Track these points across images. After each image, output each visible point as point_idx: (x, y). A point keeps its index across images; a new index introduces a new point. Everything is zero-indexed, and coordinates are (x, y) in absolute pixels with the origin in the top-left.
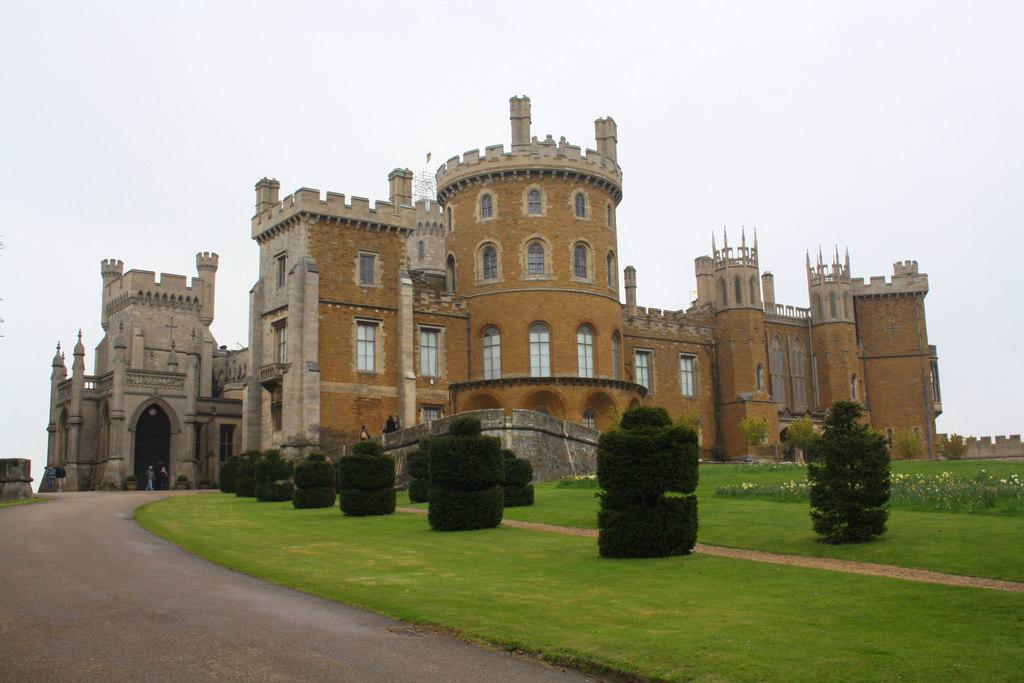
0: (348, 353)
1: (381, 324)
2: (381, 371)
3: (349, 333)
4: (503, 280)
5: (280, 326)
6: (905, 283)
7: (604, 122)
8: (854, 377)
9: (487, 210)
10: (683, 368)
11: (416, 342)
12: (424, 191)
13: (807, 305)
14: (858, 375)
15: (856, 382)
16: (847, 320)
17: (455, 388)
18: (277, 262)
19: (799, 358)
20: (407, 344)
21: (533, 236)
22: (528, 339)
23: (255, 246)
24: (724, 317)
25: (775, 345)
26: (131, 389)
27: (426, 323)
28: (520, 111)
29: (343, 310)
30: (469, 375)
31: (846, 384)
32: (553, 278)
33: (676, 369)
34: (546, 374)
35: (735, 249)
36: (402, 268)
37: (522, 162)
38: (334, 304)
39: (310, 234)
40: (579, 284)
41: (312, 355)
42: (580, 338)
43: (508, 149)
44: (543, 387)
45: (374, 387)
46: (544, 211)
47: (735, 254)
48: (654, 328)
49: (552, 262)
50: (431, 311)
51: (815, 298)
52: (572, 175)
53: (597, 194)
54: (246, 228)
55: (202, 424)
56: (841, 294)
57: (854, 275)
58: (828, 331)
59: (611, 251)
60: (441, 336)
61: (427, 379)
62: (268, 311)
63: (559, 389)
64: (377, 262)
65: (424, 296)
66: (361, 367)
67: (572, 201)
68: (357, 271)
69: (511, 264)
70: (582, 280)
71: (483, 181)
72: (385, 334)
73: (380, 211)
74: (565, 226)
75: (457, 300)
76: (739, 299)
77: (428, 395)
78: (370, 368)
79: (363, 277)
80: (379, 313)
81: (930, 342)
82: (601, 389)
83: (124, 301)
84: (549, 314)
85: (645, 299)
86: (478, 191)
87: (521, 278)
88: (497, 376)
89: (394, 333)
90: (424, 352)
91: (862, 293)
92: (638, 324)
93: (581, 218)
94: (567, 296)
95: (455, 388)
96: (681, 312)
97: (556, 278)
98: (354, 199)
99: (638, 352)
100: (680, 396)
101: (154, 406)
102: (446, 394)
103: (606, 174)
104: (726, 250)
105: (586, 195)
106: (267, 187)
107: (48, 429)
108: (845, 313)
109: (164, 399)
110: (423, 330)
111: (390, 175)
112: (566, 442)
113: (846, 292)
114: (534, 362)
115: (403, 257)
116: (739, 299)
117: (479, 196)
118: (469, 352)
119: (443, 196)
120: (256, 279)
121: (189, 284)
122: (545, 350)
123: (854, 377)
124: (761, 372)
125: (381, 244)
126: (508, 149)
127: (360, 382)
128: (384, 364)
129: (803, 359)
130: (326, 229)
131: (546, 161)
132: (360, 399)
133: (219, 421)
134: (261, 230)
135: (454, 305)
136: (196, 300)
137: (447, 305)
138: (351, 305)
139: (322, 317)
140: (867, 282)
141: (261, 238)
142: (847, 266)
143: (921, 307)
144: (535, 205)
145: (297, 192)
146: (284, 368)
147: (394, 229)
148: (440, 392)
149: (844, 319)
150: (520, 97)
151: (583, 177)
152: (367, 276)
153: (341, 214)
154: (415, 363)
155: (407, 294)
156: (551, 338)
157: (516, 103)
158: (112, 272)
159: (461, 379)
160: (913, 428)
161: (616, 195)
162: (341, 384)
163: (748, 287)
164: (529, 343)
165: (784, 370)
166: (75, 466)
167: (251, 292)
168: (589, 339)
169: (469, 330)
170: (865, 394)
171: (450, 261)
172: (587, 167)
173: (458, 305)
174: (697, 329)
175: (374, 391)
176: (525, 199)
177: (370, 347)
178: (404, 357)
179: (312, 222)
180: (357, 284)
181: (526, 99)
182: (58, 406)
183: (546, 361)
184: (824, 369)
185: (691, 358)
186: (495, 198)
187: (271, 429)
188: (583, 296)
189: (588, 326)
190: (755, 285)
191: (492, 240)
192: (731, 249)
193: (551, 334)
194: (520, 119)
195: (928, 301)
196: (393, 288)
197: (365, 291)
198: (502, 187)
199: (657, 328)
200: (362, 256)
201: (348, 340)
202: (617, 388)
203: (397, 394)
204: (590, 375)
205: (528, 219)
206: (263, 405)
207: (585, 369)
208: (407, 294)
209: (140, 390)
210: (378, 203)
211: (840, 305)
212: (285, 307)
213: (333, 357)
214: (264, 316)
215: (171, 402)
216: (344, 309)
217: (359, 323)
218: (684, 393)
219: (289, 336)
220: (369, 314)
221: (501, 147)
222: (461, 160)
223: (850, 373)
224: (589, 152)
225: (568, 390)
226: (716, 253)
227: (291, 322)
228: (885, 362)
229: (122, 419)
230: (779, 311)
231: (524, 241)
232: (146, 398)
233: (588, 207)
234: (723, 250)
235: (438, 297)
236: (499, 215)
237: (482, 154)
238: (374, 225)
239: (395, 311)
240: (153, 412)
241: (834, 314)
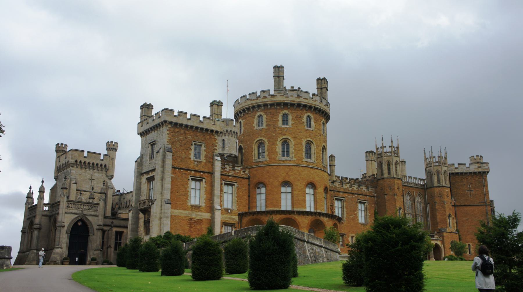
0: (186, 195)
1: (204, 180)
2: (203, 205)
3: (187, 184)
4: (268, 159)
5: (150, 180)
6: (477, 167)
7: (321, 80)
8: (450, 215)
9: (260, 123)
10: (360, 208)
11: (221, 190)
12: (228, 112)
13: (424, 177)
14: (451, 214)
15: (451, 218)
16: (446, 185)
17: (241, 215)
18: (150, 147)
19: (420, 204)
20: (217, 192)
21: (284, 137)
22: (280, 191)
23: (139, 138)
24: (381, 182)
25: (408, 197)
26: (69, 211)
27: (227, 181)
28: (279, 72)
29: (184, 171)
30: (249, 208)
31: (445, 219)
32: (294, 159)
33: (356, 209)
34: (289, 209)
35: (387, 147)
37: (279, 99)
38: (180, 169)
39: (168, 132)
40: (308, 162)
41: (167, 195)
42: (308, 190)
43: (272, 92)
44: (288, 216)
45: (198, 213)
47: (388, 150)
48: (345, 187)
49: (293, 151)
50: (230, 174)
51: (429, 174)
52: (305, 106)
53: (317, 116)
54: (135, 128)
55: (106, 230)
56: (443, 172)
57: (449, 162)
58: (436, 191)
59: (324, 146)
60: (235, 187)
61: (227, 210)
62: (144, 171)
63: (296, 217)
64: (203, 148)
65: (227, 166)
66: (192, 202)
67: (304, 120)
68: (192, 152)
69: (272, 151)
70: (309, 160)
71: (259, 109)
72: (206, 186)
73: (205, 122)
74: (300, 132)
75: (244, 169)
76: (389, 173)
77: (227, 218)
78: (197, 203)
79: (195, 155)
80: (203, 175)
81: (491, 199)
82: (318, 217)
83: (67, 165)
85: (340, 171)
86: (256, 113)
87: (277, 159)
88: (263, 209)
89: (212, 185)
90: (225, 196)
91: (453, 172)
92: (337, 184)
93: (309, 129)
94: (302, 169)
95: (241, 215)
96: (358, 179)
97: (296, 159)
98: (192, 115)
99: (336, 199)
100: (358, 223)
101: (81, 220)
102: (236, 218)
103: (322, 106)
104: (383, 147)
105: (312, 117)
106: (146, 107)
107: (21, 231)
108: (445, 181)
109: (87, 217)
110: (225, 184)
111: (211, 104)
112: (306, 244)
113: (445, 171)
114: (283, 202)
115: (216, 146)
116: (389, 173)
117: (257, 116)
118: (249, 196)
119: (237, 115)
120: (138, 155)
121: (102, 158)
122: (289, 196)
123: (450, 215)
124: (401, 211)
125: (205, 138)
126: (272, 92)
127: (192, 210)
128: (204, 201)
129: (422, 205)
130: (177, 130)
131: (292, 98)
132: (191, 219)
133: (115, 229)
134: (142, 130)
136: (105, 166)
137: (238, 171)
138: (187, 170)
139: (173, 175)
141: (143, 134)
142: (446, 158)
143: (486, 180)
145: (162, 111)
146: (152, 202)
147: (212, 131)
148: (233, 217)
149: (444, 185)
150: (279, 66)
151: (310, 107)
152: (198, 155)
153: (185, 122)
154: (221, 201)
155: (218, 165)
156: (292, 190)
157: (277, 69)
158: (61, 150)
159: (245, 210)
161: (327, 117)
162: (182, 211)
163: (394, 167)
164: (281, 193)
165: (412, 211)
166: (35, 251)
167: (136, 162)
168: (312, 191)
169: (249, 185)
170: (455, 225)
171: (240, 149)
172: (312, 102)
173: (244, 172)
174: (367, 188)
175: (199, 215)
176: (280, 118)
177: (198, 192)
178: (215, 198)
179: (170, 126)
180: (192, 159)
181: (282, 67)
182: (28, 219)
183: (289, 202)
184: (434, 211)
185: (364, 203)
186: (265, 117)
187: (143, 234)
188: (309, 169)
189: (312, 185)
191: (262, 138)
192: (385, 147)
193: (292, 188)
194: (279, 77)
195: (489, 176)
196: (211, 161)
197: (196, 163)
198: (269, 111)
199: (347, 186)
200: (195, 144)
201: (186, 188)
202: (326, 217)
203: (211, 217)
204: (312, 210)
205: (281, 129)
206: (140, 221)
207: (310, 207)
208: (218, 165)
209: (74, 211)
210: (204, 117)
211: (442, 177)
212: (154, 170)
213: (178, 197)
214: (142, 174)
215: (90, 218)
216: (185, 172)
217: (192, 179)
218: (360, 221)
219: (156, 185)
220: (198, 175)
221: (269, 91)
222: (248, 97)
223: (447, 215)
224: (313, 95)
225: (300, 217)
226: (377, 149)
227: (158, 177)
228: (466, 208)
229: (63, 227)
230: (407, 180)
231: (279, 139)
232: (76, 216)
233: (313, 123)
234: (381, 148)
235: (234, 167)
236: (266, 126)
237: (259, 94)
238: (202, 129)
240: (80, 223)
241: (439, 182)
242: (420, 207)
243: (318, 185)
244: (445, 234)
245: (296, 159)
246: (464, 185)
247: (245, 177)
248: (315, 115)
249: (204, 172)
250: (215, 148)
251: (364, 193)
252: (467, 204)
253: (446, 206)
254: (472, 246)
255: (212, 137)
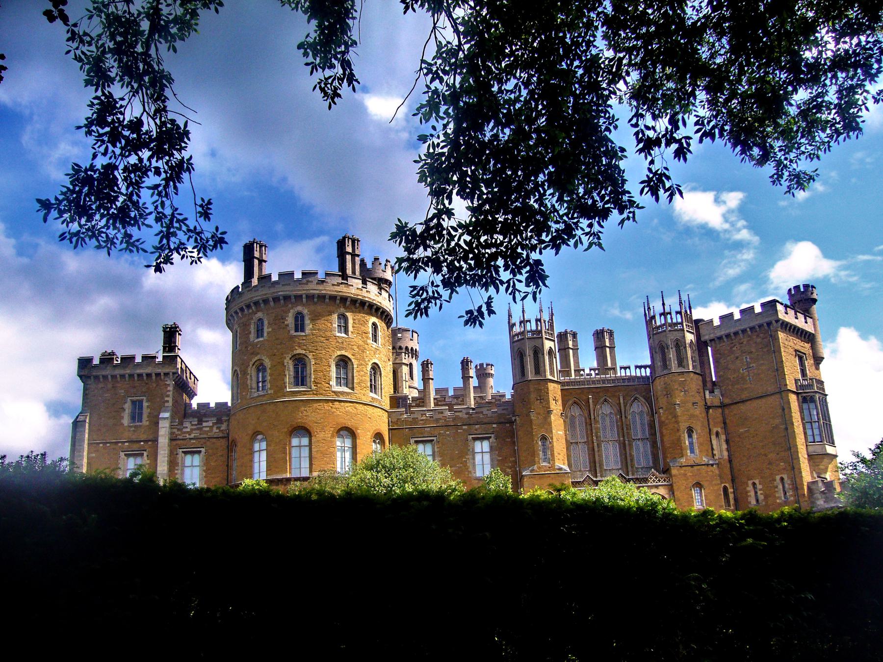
1: (145, 454)
8: (690, 431)
36: (166, 404)
38: (105, 443)
42: (295, 441)
46: (265, 334)
50: (192, 436)
64: (145, 404)
67: (290, 320)
79: (133, 418)
84: (265, 424)
118: (228, 466)
125: (148, 388)
130: (101, 385)
135: (215, 429)
137: (208, 429)
140: (717, 322)
144: (260, 332)
160: (778, 478)
170: (725, 446)
180: (126, 424)
185: (488, 438)
190: (540, 355)
216: (113, 446)
220: (135, 446)
223: (684, 426)
228: (742, 407)
239: (155, 441)
242: (642, 424)
243: (314, 429)
244: (674, 471)
245: (272, 391)
246: (737, 358)
247: (221, 435)
248: (313, 307)
249: (146, 441)
250: (166, 399)
251: (485, 421)
252: (744, 396)
253: (678, 410)
254: (759, 487)
255: (162, 383)
